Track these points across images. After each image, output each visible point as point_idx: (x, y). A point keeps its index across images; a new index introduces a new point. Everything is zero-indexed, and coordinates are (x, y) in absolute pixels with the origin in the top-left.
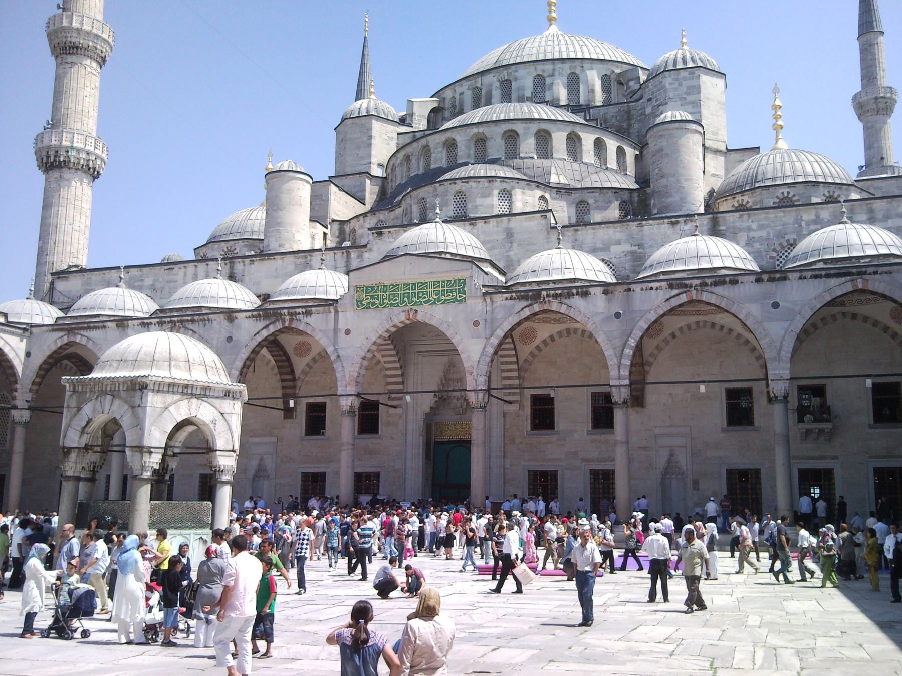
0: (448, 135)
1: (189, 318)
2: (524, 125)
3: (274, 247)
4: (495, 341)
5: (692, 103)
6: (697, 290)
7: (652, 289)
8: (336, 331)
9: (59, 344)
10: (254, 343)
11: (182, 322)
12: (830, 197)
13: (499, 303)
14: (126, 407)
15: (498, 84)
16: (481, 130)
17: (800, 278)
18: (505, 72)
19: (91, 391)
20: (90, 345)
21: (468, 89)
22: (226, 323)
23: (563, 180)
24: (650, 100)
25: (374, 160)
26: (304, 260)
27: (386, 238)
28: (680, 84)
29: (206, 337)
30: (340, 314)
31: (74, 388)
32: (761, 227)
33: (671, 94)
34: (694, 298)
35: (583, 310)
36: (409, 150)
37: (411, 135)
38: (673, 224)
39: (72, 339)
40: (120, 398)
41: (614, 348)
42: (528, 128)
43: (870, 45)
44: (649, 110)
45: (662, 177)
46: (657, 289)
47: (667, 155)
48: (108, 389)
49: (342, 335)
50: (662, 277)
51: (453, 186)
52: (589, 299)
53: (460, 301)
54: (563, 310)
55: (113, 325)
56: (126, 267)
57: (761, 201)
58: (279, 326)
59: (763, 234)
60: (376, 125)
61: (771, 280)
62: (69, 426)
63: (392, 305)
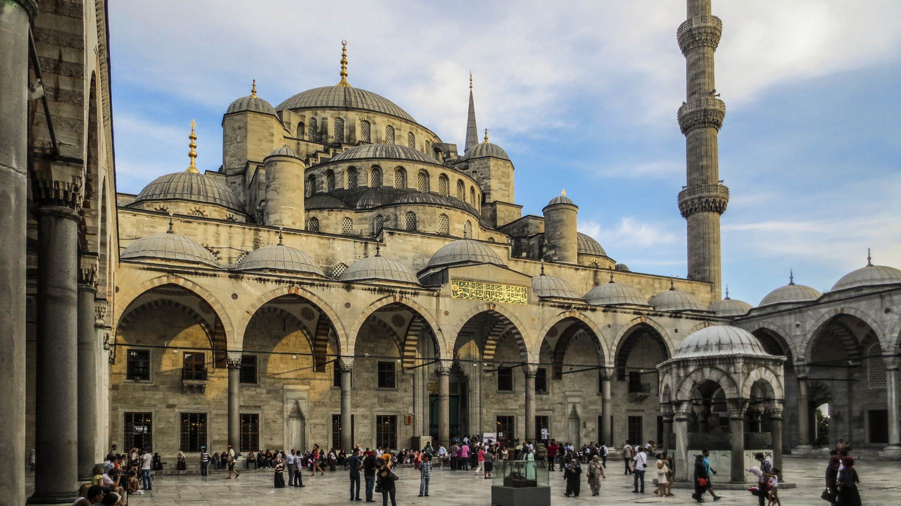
0: (399, 164)
1: (310, 282)
3: (288, 222)
5: (504, 183)
8: (438, 311)
9: (157, 283)
10: (369, 312)
11: (300, 283)
16: (425, 167)
20: (197, 290)
22: (344, 291)
26: (326, 242)
33: (493, 173)
38: (577, 269)
39: (173, 280)
45: (563, 238)
47: (567, 225)
49: (442, 315)
55: (228, 274)
58: (391, 300)
62: (744, 385)
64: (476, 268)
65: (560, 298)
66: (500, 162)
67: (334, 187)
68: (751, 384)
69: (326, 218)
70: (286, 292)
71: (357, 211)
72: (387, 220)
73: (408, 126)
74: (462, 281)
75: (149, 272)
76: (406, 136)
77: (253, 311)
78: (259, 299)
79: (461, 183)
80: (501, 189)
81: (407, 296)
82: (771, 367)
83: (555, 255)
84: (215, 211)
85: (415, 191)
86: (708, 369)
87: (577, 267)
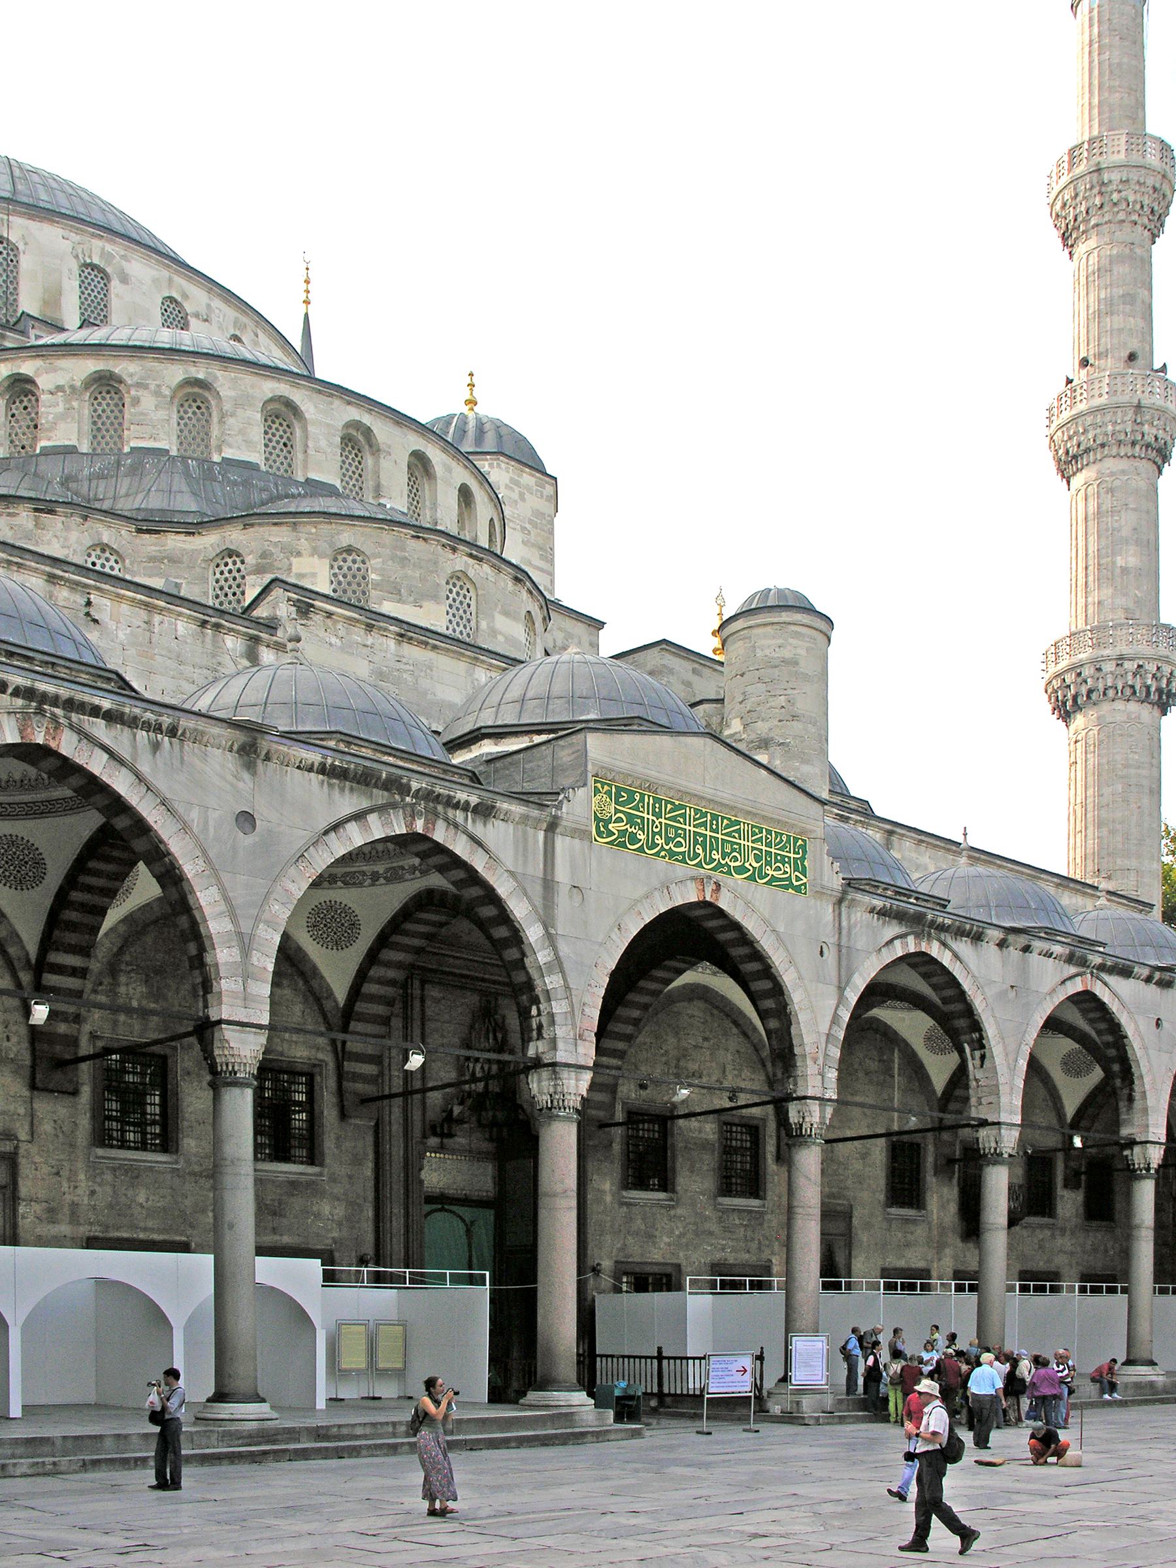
6: (1092, 974)
8: (549, 884)
11: (71, 705)
22: (231, 762)
29: (160, 783)
49: (564, 902)
53: (797, 889)
54: (946, 959)
63: (671, 854)
81: (450, 813)
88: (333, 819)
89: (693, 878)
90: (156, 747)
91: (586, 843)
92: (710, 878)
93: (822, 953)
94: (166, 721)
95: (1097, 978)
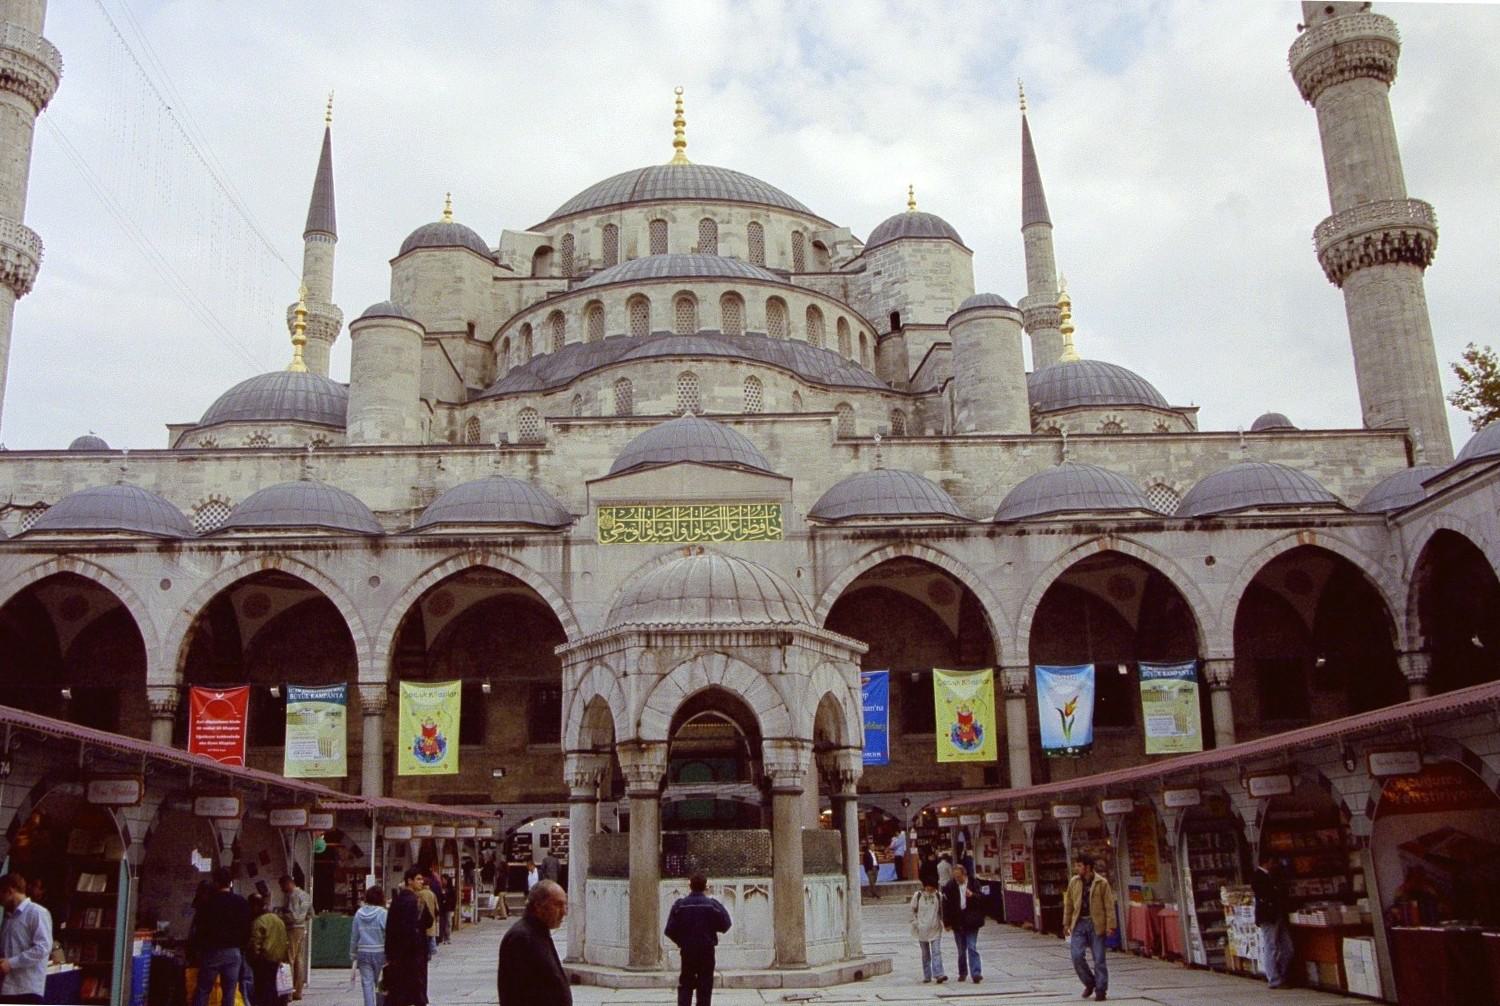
1: (300, 543)
2: (752, 288)
3: (372, 436)
4: (830, 599)
6: (1111, 537)
7: (1053, 532)
8: (566, 575)
9: (40, 574)
10: (418, 590)
11: (285, 548)
12: (1161, 426)
13: (833, 543)
14: (755, 673)
15: (647, 224)
16: (688, 287)
17: (1240, 527)
18: (658, 208)
19: (681, 647)
20: (104, 580)
21: (597, 225)
23: (814, 374)
24: (879, 273)
25: (463, 316)
27: (574, 433)
28: (923, 258)
29: (329, 574)
30: (574, 551)
31: (648, 642)
32: (1121, 459)
33: (911, 270)
34: (1109, 548)
35: (961, 559)
36: (563, 306)
37: (518, 282)
39: (66, 568)
40: (741, 659)
41: (1005, 615)
42: (758, 292)
43: (1039, 239)
44: (876, 288)
45: (980, 381)
46: (1060, 533)
47: (987, 352)
48: (717, 643)
49: (577, 585)
50: (1060, 517)
51: (678, 364)
52: (971, 542)
54: (930, 556)
55: (154, 545)
56: (132, 452)
57: (1081, 426)
58: (464, 563)
59: (1123, 467)
60: (465, 260)
61: (1204, 528)
63: (660, 538)
64: (650, 474)
65: (875, 517)
66: (927, 245)
67: (531, 353)
68: (675, 702)
69: (492, 415)
70: (257, 567)
71: (549, 391)
72: (586, 402)
73: (745, 211)
74: (623, 508)
75: (31, 556)
76: (743, 231)
77: (197, 608)
78: (208, 583)
79: (776, 304)
80: (933, 297)
81: (498, 550)
82: (748, 654)
83: (969, 419)
84: (290, 432)
85: (666, 335)
86: (599, 667)
87: (1010, 442)
88: (424, 569)
89: (680, 549)
90: (328, 556)
91: (594, 546)
92: (694, 546)
93: (799, 574)
94: (330, 543)
95: (1119, 538)
